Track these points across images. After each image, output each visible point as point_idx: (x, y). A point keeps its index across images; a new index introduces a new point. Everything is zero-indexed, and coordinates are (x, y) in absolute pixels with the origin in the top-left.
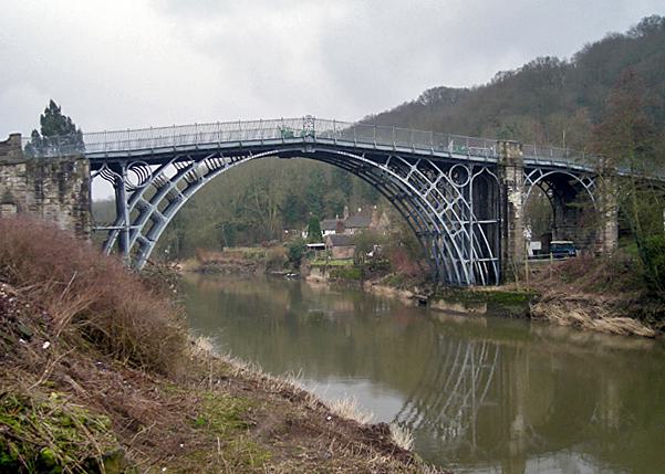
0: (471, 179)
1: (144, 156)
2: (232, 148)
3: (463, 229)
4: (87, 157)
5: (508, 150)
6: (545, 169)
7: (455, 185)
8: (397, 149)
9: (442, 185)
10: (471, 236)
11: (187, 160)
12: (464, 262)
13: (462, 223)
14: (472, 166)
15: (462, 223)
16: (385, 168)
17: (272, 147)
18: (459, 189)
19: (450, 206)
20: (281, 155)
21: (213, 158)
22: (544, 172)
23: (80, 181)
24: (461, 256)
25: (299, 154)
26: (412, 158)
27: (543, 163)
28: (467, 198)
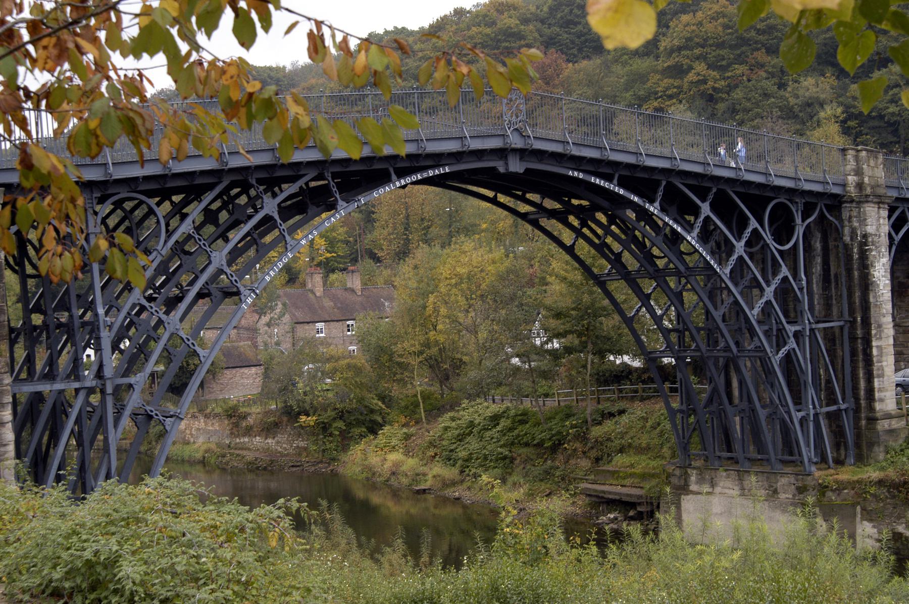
0: (800, 230)
3: (792, 344)
5: (865, 166)
12: (797, 416)
13: (791, 329)
14: (800, 201)
15: (791, 329)
17: (437, 159)
18: (780, 252)
19: (769, 292)
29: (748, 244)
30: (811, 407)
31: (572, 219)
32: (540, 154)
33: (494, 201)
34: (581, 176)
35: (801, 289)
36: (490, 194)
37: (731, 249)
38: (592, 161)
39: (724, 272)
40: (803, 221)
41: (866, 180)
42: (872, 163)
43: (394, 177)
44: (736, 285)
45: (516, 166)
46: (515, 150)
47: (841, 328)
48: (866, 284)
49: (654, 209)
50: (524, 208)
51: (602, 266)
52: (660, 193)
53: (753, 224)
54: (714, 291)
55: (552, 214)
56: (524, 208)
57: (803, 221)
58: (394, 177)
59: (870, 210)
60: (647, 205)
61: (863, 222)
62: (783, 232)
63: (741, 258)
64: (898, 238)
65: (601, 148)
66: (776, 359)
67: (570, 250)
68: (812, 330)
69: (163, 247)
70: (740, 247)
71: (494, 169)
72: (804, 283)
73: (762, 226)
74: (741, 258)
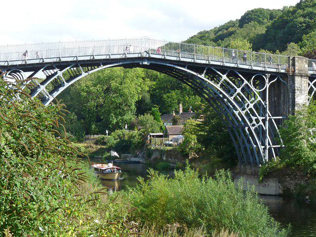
0: (267, 85)
1: (19, 65)
3: (261, 123)
5: (296, 63)
8: (212, 63)
9: (246, 90)
11: (53, 68)
13: (261, 118)
14: (268, 75)
16: (202, 76)
20: (125, 66)
21: (73, 67)
24: (259, 143)
25: (138, 65)
26: (223, 69)
28: (264, 99)
30: (267, 145)
34: (172, 66)
35: (266, 105)
41: (296, 68)
42: (300, 62)
52: (205, 71)
57: (269, 82)
59: (298, 80)
60: (199, 76)
68: (270, 120)
72: (267, 103)
73: (250, 83)
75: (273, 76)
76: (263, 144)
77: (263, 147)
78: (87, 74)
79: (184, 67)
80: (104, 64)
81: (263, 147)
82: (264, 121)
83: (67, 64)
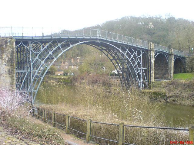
0: (141, 54)
1: (39, 39)
2: (74, 39)
4: (14, 38)
6: (158, 52)
7: (137, 56)
10: (141, 73)
13: (139, 69)
15: (139, 69)
17: (86, 40)
18: (138, 57)
19: (136, 63)
22: (158, 53)
23: (11, 50)
26: (127, 46)
27: (158, 50)
29: (134, 56)
31: (107, 51)
32: (102, 40)
33: (96, 47)
34: (109, 44)
36: (95, 46)
37: (131, 56)
38: (110, 41)
39: (130, 60)
40: (142, 52)
43: (79, 42)
44: (131, 62)
45: (99, 42)
46: (98, 39)
47: (147, 69)
48: (151, 63)
49: (120, 49)
50: (100, 49)
51: (112, 58)
53: (134, 53)
54: (129, 63)
55: (104, 50)
56: (100, 49)
57: (142, 52)
58: (79, 42)
59: (152, 52)
61: (151, 53)
62: (139, 54)
63: (132, 58)
64: (155, 57)
65: (112, 40)
66: (137, 73)
67: (107, 55)
69: (42, 50)
70: (132, 56)
71: (95, 42)
73: (136, 52)
74: (132, 58)
75: (143, 50)
76: (140, 79)
77: (140, 82)
78: (72, 46)
79: (113, 44)
80: (80, 42)
81: (140, 82)
82: (140, 70)
83: (62, 40)
